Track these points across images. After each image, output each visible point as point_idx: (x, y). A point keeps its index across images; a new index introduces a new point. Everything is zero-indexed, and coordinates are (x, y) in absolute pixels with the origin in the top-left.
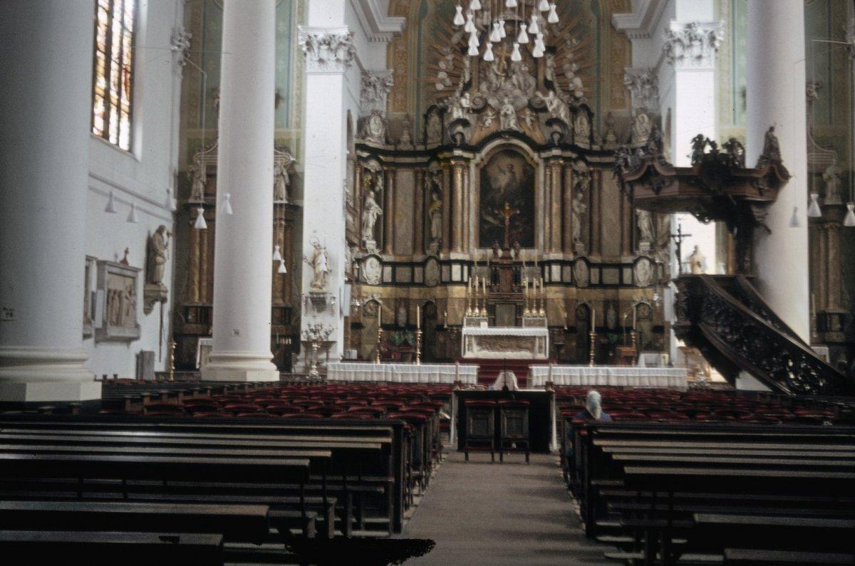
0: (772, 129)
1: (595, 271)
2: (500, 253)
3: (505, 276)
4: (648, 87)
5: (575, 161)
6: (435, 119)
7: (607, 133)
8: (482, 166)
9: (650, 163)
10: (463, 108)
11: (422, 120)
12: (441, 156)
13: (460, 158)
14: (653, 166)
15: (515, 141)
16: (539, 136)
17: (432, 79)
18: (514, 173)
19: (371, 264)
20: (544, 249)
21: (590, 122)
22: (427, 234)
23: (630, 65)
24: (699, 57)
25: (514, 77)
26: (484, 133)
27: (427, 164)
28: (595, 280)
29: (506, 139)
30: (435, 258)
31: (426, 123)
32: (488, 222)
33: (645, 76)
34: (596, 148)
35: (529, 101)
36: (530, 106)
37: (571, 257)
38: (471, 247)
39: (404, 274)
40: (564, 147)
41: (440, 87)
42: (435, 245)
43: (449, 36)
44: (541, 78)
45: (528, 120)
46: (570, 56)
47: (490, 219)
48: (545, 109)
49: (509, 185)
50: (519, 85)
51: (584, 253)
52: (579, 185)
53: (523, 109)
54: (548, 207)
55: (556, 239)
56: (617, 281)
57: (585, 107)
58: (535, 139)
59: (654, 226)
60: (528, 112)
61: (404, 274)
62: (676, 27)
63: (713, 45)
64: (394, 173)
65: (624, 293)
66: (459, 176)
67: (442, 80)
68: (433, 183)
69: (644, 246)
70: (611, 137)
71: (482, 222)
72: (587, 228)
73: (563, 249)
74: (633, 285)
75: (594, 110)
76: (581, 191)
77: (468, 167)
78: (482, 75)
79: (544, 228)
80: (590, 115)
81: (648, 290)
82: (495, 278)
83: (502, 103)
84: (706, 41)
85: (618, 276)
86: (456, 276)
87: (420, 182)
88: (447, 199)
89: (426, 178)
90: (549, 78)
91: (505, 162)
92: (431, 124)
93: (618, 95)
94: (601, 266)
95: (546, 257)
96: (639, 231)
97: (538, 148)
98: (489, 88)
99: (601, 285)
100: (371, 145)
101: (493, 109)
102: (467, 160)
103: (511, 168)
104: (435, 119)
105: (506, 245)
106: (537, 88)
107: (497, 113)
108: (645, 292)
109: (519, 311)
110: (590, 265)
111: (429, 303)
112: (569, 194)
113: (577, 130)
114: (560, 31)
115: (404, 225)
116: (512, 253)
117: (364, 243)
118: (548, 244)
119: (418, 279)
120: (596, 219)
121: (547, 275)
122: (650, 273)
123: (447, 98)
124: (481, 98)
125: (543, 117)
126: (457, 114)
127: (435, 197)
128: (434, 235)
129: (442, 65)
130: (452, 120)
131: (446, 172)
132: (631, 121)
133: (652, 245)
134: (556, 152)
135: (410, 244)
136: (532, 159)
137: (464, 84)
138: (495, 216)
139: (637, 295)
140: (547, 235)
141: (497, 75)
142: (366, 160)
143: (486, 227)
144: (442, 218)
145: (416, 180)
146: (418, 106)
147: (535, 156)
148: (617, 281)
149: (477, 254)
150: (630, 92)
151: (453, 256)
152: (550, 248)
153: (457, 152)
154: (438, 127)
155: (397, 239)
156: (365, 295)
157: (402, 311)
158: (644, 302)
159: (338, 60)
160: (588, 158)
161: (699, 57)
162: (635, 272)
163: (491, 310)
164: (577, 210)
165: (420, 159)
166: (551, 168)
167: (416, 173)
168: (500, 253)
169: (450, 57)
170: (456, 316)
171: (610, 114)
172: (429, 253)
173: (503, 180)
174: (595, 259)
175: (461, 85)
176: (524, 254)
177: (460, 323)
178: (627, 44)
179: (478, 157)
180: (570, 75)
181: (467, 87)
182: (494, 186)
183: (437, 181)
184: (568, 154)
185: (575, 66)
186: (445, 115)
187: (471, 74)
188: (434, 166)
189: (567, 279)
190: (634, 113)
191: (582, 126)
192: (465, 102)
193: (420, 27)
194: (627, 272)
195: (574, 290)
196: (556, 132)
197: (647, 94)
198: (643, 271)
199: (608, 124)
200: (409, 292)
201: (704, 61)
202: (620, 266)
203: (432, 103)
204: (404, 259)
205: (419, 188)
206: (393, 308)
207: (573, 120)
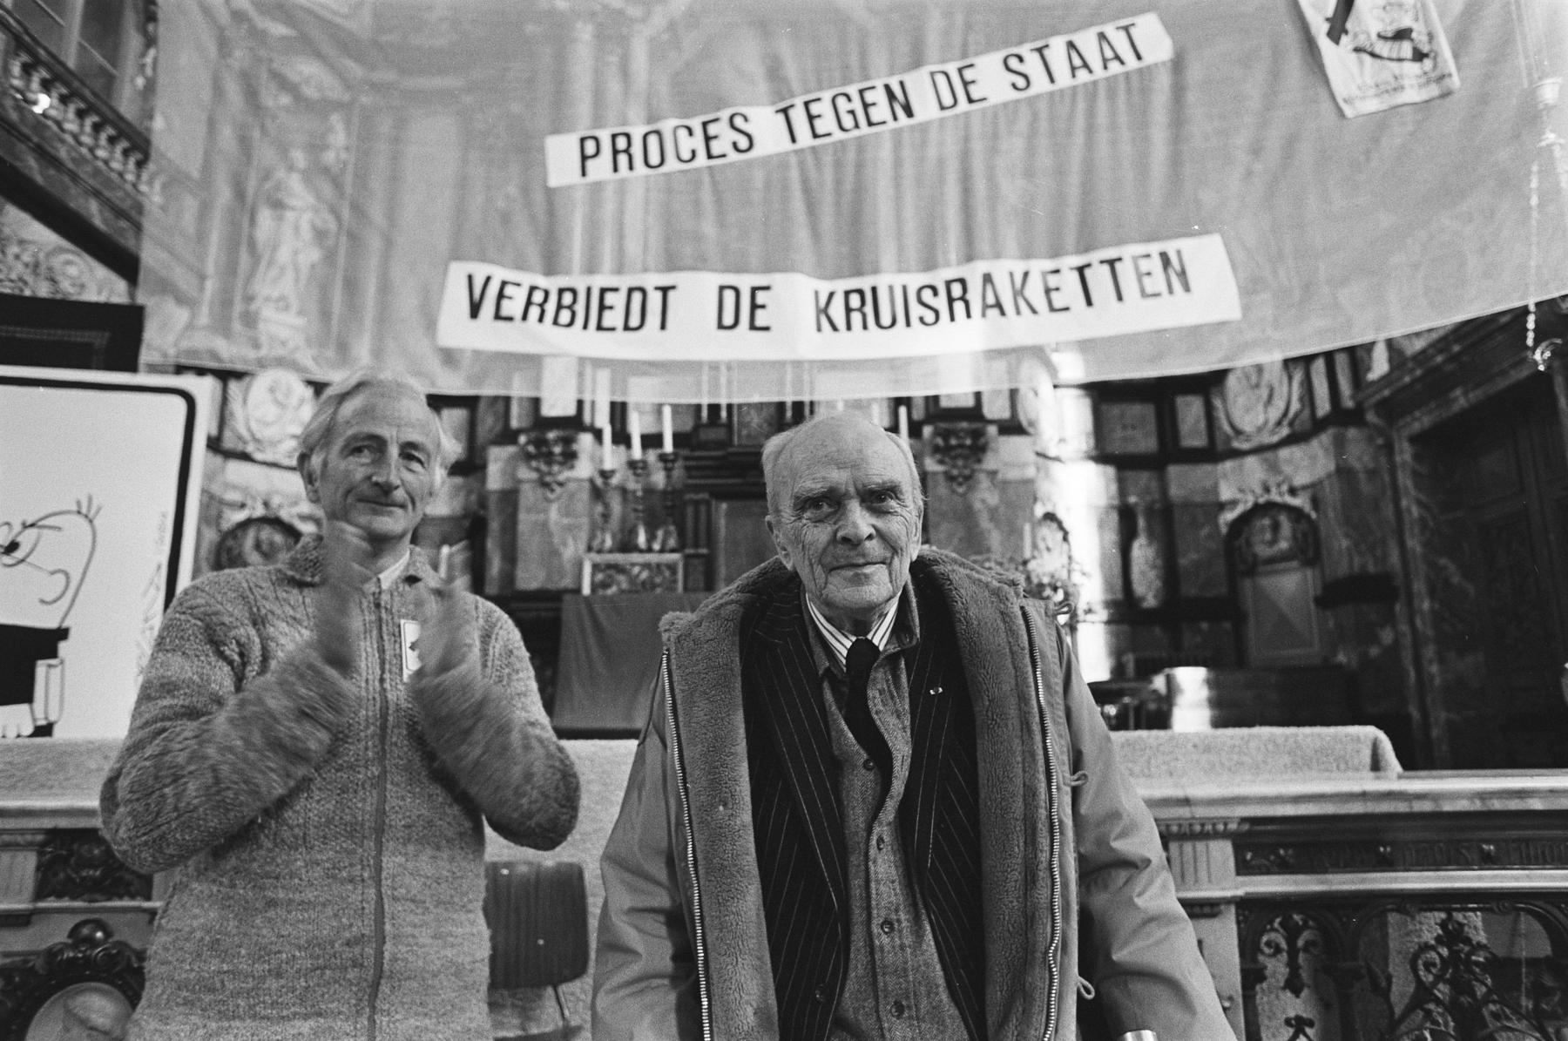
19: (272, 390)
56: (1146, 442)
64: (401, 123)
74: (1216, 450)
77: (624, 41)
81: (1284, 453)
85: (1152, 426)
108: (1274, 468)
117: (250, 320)
139: (1238, 485)
156: (233, 496)
158: (1275, 497)
162: (1217, 403)
170: (551, 554)
177: (567, 582)
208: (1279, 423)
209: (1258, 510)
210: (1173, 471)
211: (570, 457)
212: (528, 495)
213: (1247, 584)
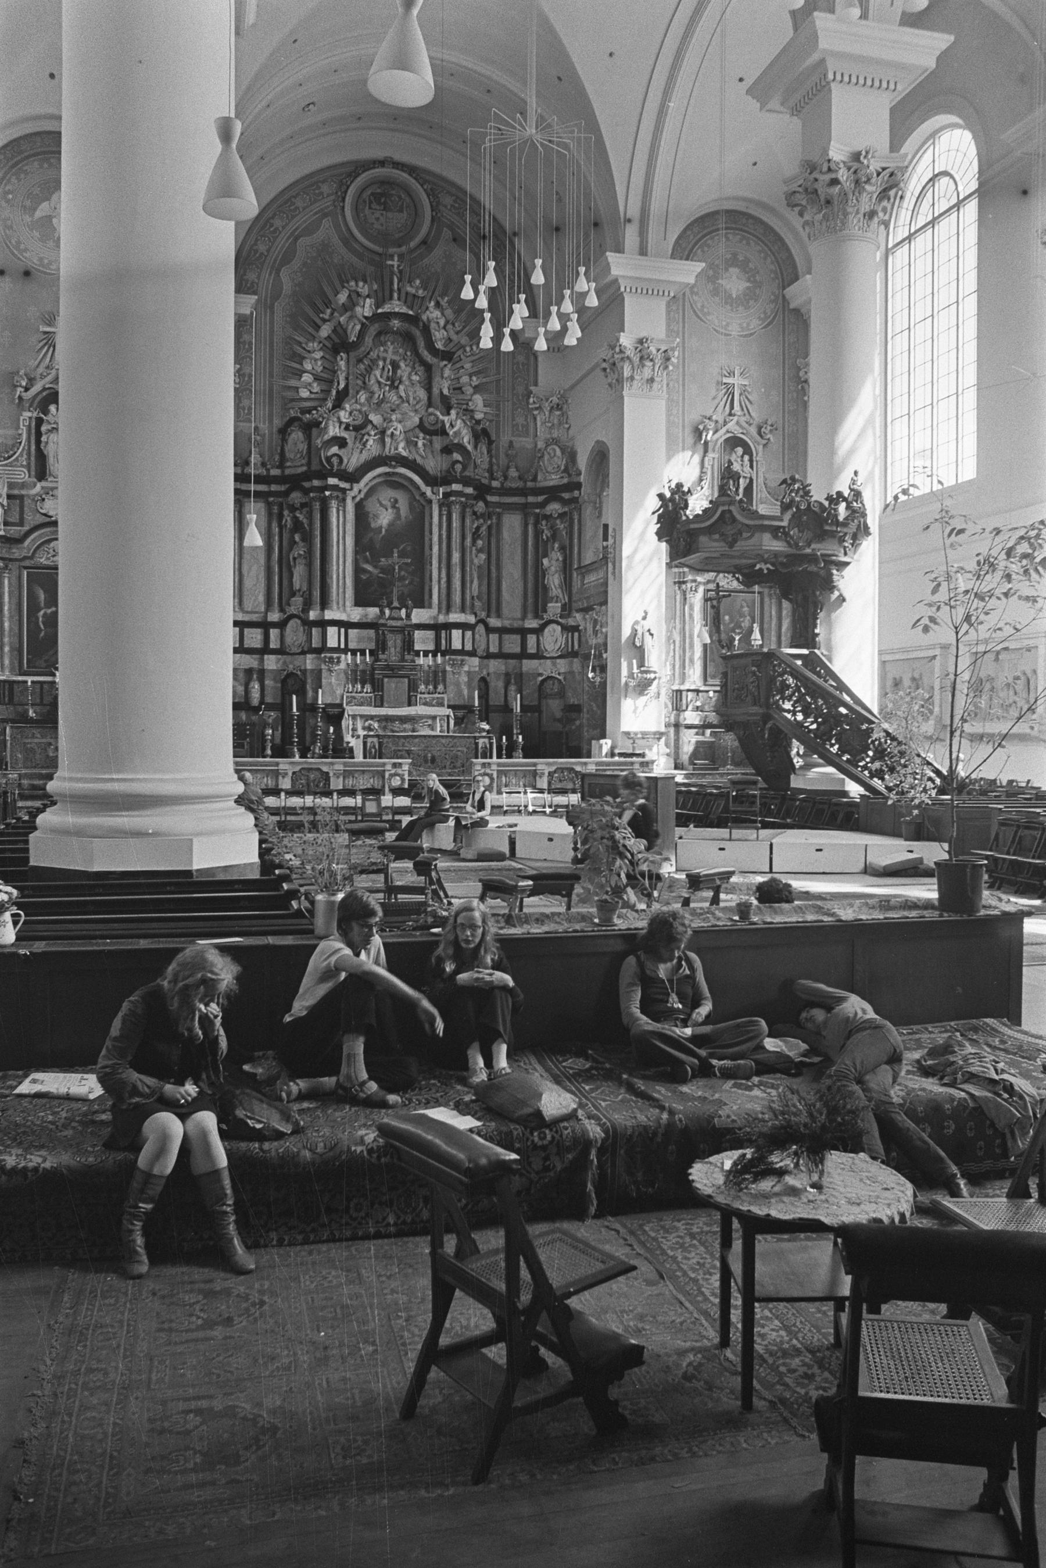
0: (856, 473)
1: (494, 638)
2: (387, 612)
3: (394, 642)
5: (477, 498)
6: (296, 436)
7: (508, 467)
8: (358, 499)
9: (726, 508)
10: (341, 423)
11: (276, 436)
12: (307, 485)
13: (335, 488)
14: (730, 511)
15: (402, 470)
16: (433, 464)
17: (293, 383)
18: (398, 509)
20: (440, 609)
21: (489, 451)
22: (285, 583)
23: (536, 384)
24: (651, 380)
25: (401, 387)
26: (365, 456)
27: (286, 494)
28: (494, 649)
29: (390, 466)
30: (299, 617)
31: (284, 440)
32: (365, 571)
33: (555, 400)
34: (495, 484)
35: (421, 419)
36: (421, 426)
37: (472, 619)
38: (348, 604)
39: (254, 638)
40: (466, 482)
41: (304, 393)
42: (298, 601)
43: (318, 328)
44: (435, 391)
45: (420, 444)
46: (468, 366)
47: (369, 567)
48: (443, 432)
49: (391, 525)
50: (408, 396)
51: (483, 615)
52: (478, 528)
53: (412, 430)
54: (444, 555)
55: (457, 598)
56: (517, 650)
57: (485, 432)
58: (428, 468)
59: (567, 583)
60: (421, 435)
61: (254, 638)
62: (626, 340)
63: (666, 367)
65: (528, 665)
66: (334, 510)
67: (307, 387)
68: (295, 520)
69: (554, 608)
70: (513, 473)
71: (358, 570)
72: (485, 582)
73: (463, 610)
74: (539, 656)
75: (493, 438)
76: (479, 537)
77: (344, 500)
78: (359, 382)
79: (439, 582)
80: (490, 442)
82: (381, 645)
83: (387, 420)
84: (658, 362)
86: (332, 643)
87: (275, 517)
88: (318, 540)
89: (286, 513)
90: (446, 392)
91: (387, 495)
92: (290, 441)
93: (520, 420)
94: (502, 631)
95: (442, 619)
96: (546, 589)
97: (432, 481)
98: (369, 400)
99: (501, 655)
101: (375, 427)
102: (344, 491)
103: (395, 504)
104: (296, 436)
105: (396, 604)
106: (430, 404)
107: (383, 433)
108: (554, 664)
109: (413, 687)
110: (489, 630)
111: (290, 675)
112: (468, 541)
113: (479, 461)
114: (457, 333)
115: (253, 573)
116: (403, 611)
118: (444, 603)
119: (274, 644)
120: (494, 575)
121: (443, 642)
122: (561, 641)
123: (315, 408)
124: (360, 411)
125: (438, 443)
126: (334, 430)
127: (297, 537)
128: (297, 585)
129: (308, 366)
130: (326, 438)
131: (317, 506)
132: (537, 455)
133: (564, 607)
134: (455, 487)
135: (261, 598)
136: (423, 494)
137: (338, 392)
138: (375, 564)
139: (546, 668)
140: (444, 591)
141: (379, 383)
143: (364, 577)
144: (310, 565)
145: (270, 514)
146: (271, 415)
147: (428, 491)
148: (517, 650)
149: (356, 614)
150: (535, 419)
151: (329, 615)
152: (449, 609)
153: (332, 481)
154: (303, 447)
155: (245, 593)
157: (256, 686)
160: (489, 498)
161: (651, 380)
163: (378, 687)
164: (476, 561)
165: (274, 488)
166: (449, 506)
167: (269, 505)
168: (387, 612)
169: (318, 355)
171: (511, 442)
172: (292, 610)
173: (384, 519)
174: (494, 622)
175: (334, 392)
176: (419, 616)
177: (338, 701)
178: (532, 358)
179: (356, 487)
180: (469, 390)
181: (342, 397)
182: (373, 525)
183: (301, 517)
184: (470, 490)
185: (475, 381)
186: (315, 431)
187: (347, 379)
188: (296, 497)
189: (468, 647)
190: (541, 445)
191: (481, 456)
192: (344, 416)
193: (272, 313)
194: (532, 639)
195: (475, 661)
196: (458, 462)
197: (556, 421)
198: (553, 639)
199: (507, 455)
200: (262, 661)
201: (655, 385)
202: (523, 632)
203: (292, 413)
204: (255, 618)
205: (275, 524)
206: (243, 681)
207: (476, 447)
209: (549, 678)
210: (524, 661)
211: (339, 662)
212: (324, 674)
213: (544, 702)
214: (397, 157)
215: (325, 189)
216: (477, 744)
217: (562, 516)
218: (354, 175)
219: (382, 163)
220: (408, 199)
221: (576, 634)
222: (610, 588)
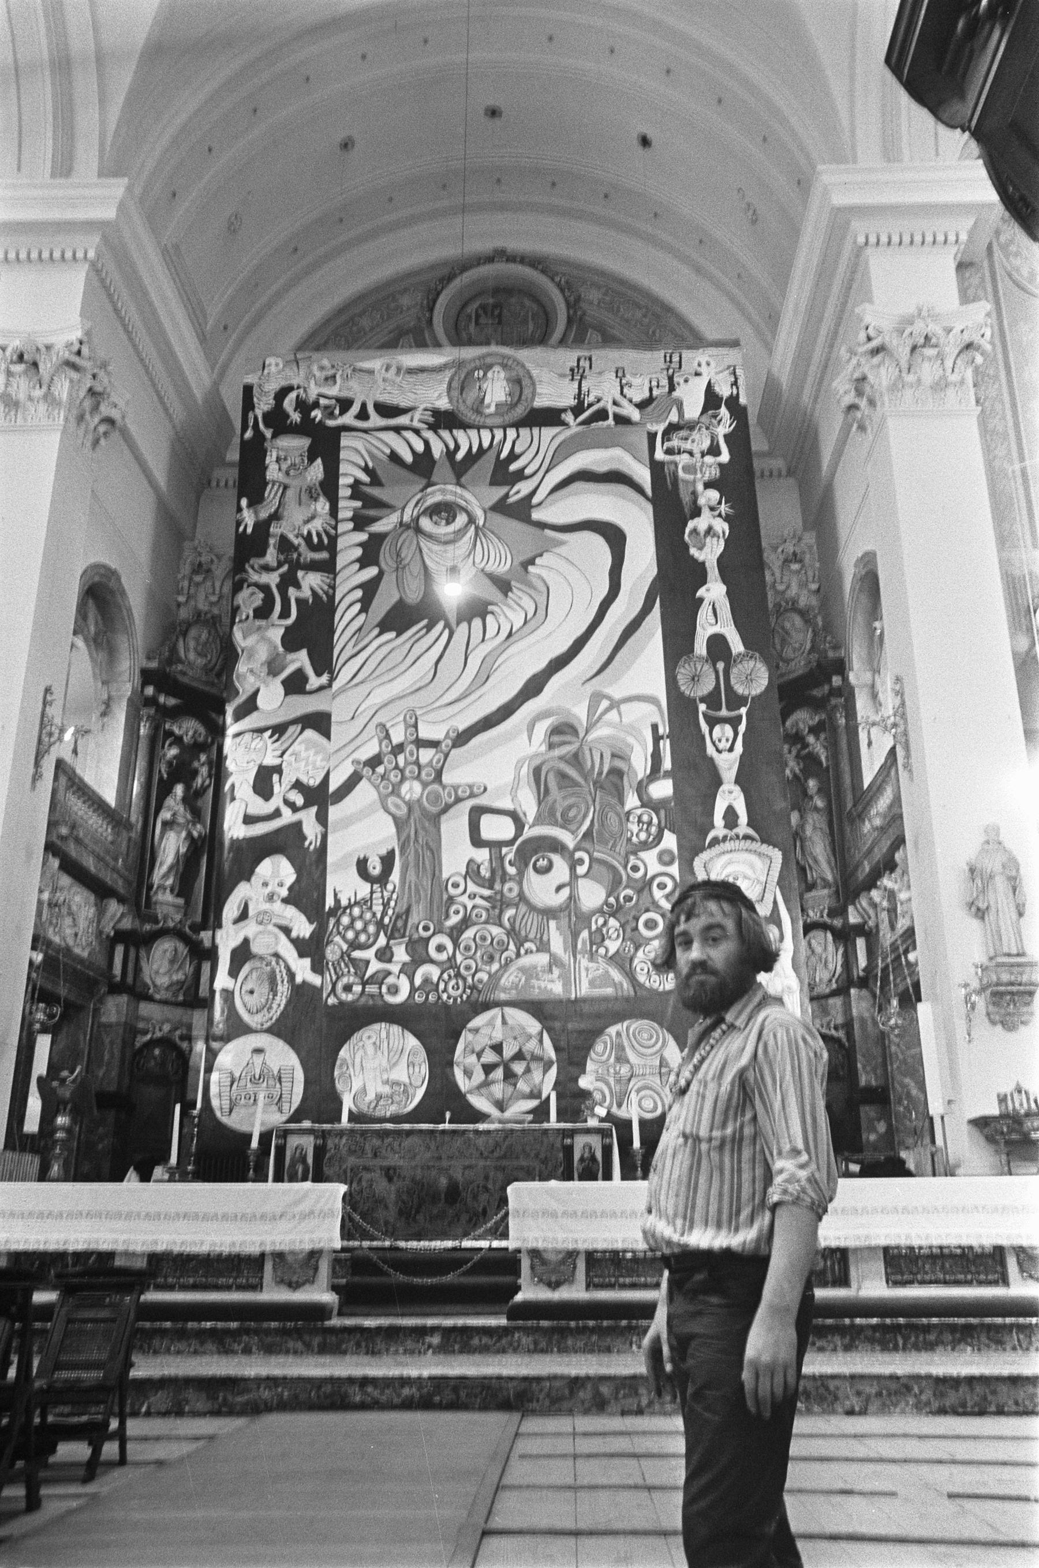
4: (795, 567)
81: (831, 1001)
100: (180, 678)
142: (174, 714)
156: (141, 1025)
159: (49, 398)
208: (830, 981)
214: (513, 245)
215: (405, 301)
216: (569, 1150)
217: (814, 730)
218: (450, 278)
219: (490, 259)
220: (535, 307)
221: (861, 943)
222: (906, 811)
